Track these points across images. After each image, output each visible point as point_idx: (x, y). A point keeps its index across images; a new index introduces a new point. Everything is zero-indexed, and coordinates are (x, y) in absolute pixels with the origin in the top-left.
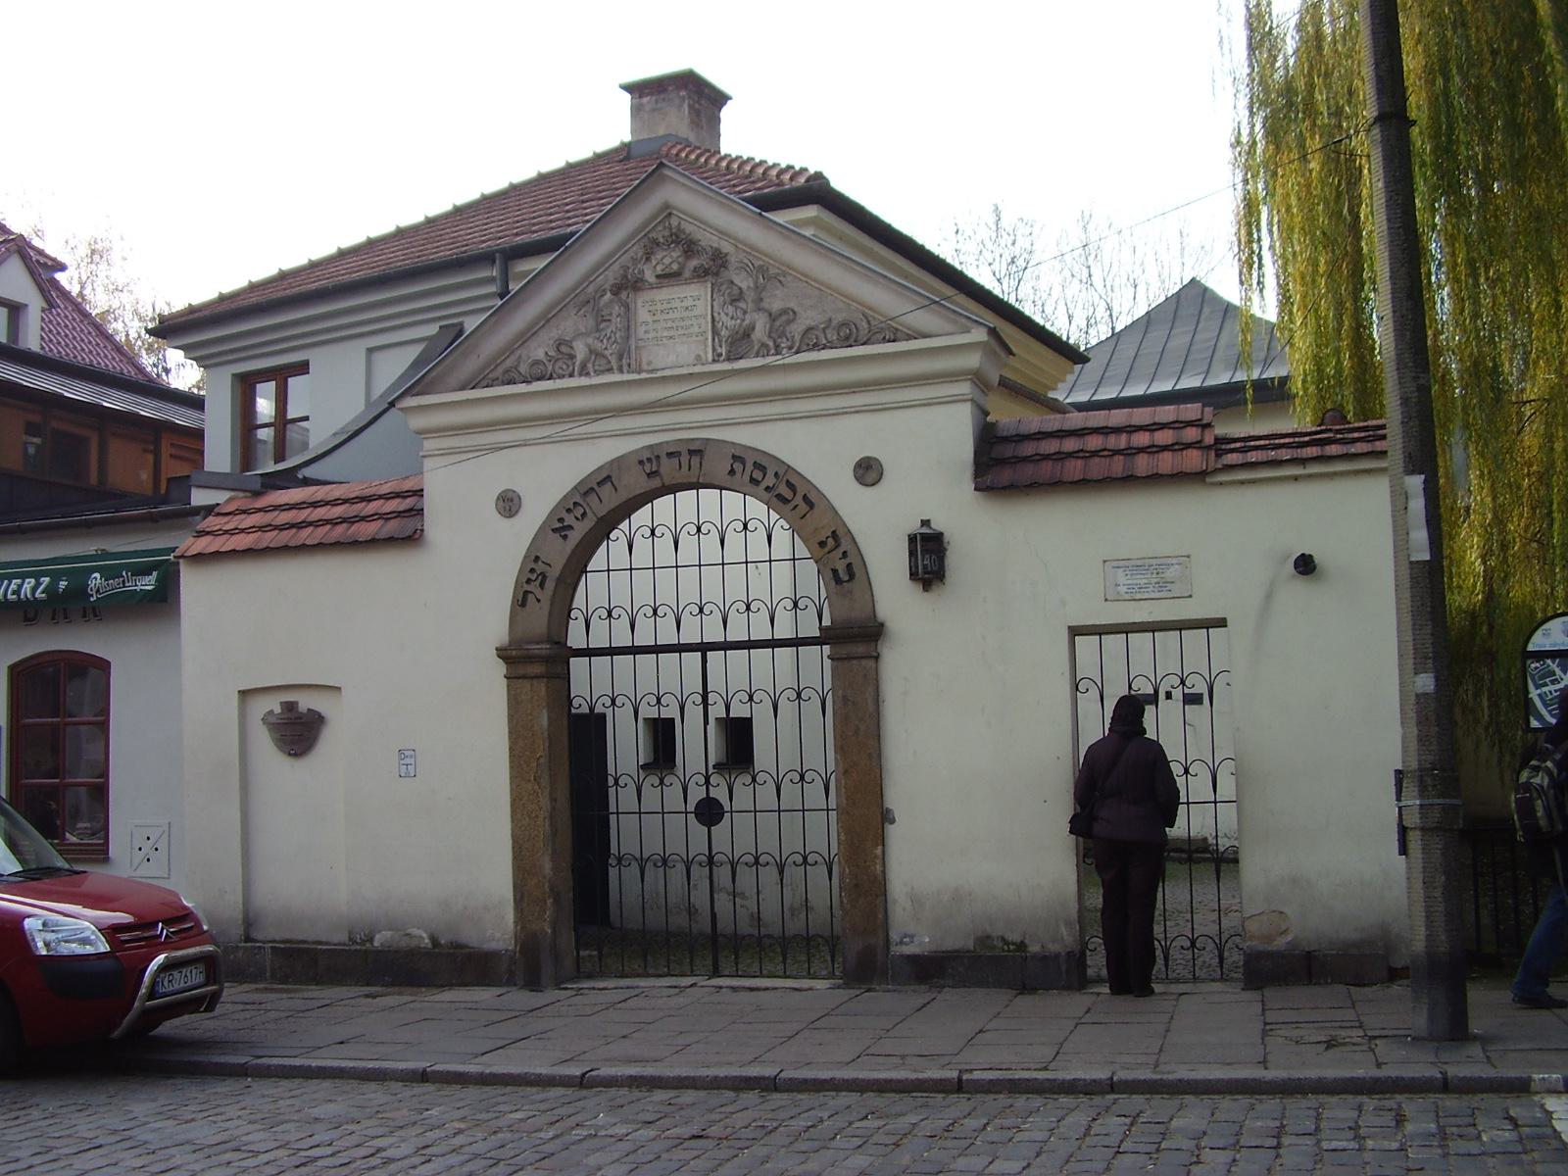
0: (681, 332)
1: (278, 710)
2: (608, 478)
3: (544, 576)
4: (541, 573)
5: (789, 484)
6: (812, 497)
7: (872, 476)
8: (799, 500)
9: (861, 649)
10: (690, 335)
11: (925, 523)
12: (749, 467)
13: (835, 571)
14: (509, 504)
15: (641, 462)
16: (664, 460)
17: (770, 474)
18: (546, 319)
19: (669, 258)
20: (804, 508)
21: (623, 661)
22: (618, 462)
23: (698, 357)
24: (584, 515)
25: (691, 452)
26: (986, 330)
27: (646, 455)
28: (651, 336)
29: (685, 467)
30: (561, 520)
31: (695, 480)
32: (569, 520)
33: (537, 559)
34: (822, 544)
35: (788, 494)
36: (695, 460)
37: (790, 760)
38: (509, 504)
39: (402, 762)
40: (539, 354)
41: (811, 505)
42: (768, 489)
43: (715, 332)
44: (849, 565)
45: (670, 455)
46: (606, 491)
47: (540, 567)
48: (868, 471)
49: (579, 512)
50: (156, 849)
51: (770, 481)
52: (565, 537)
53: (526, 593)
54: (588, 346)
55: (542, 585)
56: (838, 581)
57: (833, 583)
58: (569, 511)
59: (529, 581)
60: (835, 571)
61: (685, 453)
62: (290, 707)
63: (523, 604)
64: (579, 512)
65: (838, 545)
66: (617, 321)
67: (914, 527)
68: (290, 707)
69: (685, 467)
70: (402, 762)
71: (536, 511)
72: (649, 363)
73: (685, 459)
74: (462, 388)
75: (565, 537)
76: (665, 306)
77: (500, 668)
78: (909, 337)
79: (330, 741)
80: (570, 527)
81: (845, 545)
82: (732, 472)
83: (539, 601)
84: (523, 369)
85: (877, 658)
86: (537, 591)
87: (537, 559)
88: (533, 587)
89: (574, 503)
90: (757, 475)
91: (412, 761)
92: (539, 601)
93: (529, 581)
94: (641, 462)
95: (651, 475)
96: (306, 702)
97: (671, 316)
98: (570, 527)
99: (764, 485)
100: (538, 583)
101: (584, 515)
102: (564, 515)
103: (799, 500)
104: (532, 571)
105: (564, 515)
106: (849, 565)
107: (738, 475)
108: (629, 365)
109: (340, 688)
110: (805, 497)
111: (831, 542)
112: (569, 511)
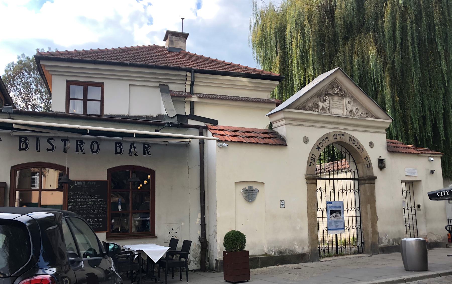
0: (339, 107)
1: (247, 188)
2: (327, 138)
3: (314, 159)
4: (314, 158)
5: (359, 145)
6: (363, 149)
7: (372, 146)
8: (361, 148)
9: (373, 182)
10: (340, 108)
11: (380, 157)
12: (353, 140)
13: (367, 165)
14: (306, 140)
15: (333, 135)
16: (337, 135)
17: (356, 142)
18: (312, 97)
19: (336, 91)
20: (362, 150)
21: (344, 181)
22: (329, 134)
23: (342, 114)
24: (323, 145)
25: (343, 135)
26: (392, 120)
27: (334, 134)
28: (333, 106)
29: (341, 138)
30: (318, 146)
31: (343, 141)
32: (320, 146)
33: (313, 155)
34: (365, 159)
35: (359, 147)
36: (343, 136)
37: (350, 206)
38: (306, 140)
39: (281, 204)
40: (310, 105)
41: (363, 150)
42: (356, 145)
43: (346, 109)
44: (369, 164)
45: (339, 135)
46: (326, 140)
47: (314, 157)
48: (371, 145)
49: (322, 144)
50: (176, 233)
51: (356, 144)
52: (319, 150)
53: (311, 163)
54: (322, 106)
55: (314, 161)
56: (368, 167)
57: (367, 167)
58: (319, 144)
59: (311, 160)
60: (367, 165)
61: (341, 135)
62: (251, 187)
63: (310, 165)
64: (322, 144)
65: (367, 160)
66: (328, 102)
67: (378, 157)
68: (251, 187)
69: (341, 138)
70: (281, 204)
71: (312, 142)
72: (333, 113)
73: (341, 136)
74: (294, 109)
75: (319, 150)
76: (336, 101)
77: (305, 181)
78: (376, 118)
79: (259, 197)
80: (320, 148)
81: (369, 160)
82: (349, 141)
83: (313, 165)
84: (307, 107)
85: (374, 183)
86: (313, 162)
87: (313, 155)
88: (312, 161)
89: (321, 143)
90: (354, 142)
91: (283, 204)
92: (313, 165)
93: (311, 160)
94: (333, 135)
95: (336, 138)
96: (255, 187)
97: (337, 103)
98: (320, 148)
99: (355, 144)
100: (313, 160)
101: (323, 145)
102: (319, 145)
103: (361, 148)
104: (312, 157)
105: (319, 145)
106: (369, 164)
107: (350, 141)
108: (330, 112)
109: (263, 183)
110: (362, 148)
111: (366, 158)
112: (319, 144)
